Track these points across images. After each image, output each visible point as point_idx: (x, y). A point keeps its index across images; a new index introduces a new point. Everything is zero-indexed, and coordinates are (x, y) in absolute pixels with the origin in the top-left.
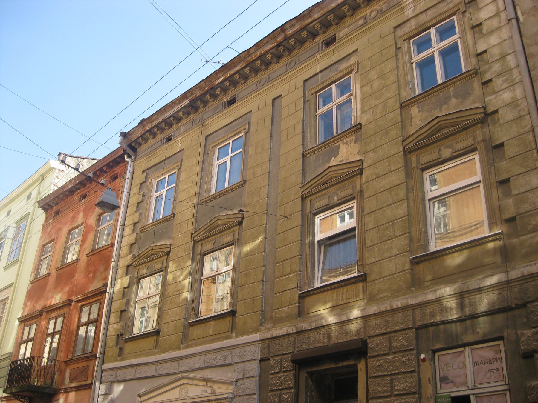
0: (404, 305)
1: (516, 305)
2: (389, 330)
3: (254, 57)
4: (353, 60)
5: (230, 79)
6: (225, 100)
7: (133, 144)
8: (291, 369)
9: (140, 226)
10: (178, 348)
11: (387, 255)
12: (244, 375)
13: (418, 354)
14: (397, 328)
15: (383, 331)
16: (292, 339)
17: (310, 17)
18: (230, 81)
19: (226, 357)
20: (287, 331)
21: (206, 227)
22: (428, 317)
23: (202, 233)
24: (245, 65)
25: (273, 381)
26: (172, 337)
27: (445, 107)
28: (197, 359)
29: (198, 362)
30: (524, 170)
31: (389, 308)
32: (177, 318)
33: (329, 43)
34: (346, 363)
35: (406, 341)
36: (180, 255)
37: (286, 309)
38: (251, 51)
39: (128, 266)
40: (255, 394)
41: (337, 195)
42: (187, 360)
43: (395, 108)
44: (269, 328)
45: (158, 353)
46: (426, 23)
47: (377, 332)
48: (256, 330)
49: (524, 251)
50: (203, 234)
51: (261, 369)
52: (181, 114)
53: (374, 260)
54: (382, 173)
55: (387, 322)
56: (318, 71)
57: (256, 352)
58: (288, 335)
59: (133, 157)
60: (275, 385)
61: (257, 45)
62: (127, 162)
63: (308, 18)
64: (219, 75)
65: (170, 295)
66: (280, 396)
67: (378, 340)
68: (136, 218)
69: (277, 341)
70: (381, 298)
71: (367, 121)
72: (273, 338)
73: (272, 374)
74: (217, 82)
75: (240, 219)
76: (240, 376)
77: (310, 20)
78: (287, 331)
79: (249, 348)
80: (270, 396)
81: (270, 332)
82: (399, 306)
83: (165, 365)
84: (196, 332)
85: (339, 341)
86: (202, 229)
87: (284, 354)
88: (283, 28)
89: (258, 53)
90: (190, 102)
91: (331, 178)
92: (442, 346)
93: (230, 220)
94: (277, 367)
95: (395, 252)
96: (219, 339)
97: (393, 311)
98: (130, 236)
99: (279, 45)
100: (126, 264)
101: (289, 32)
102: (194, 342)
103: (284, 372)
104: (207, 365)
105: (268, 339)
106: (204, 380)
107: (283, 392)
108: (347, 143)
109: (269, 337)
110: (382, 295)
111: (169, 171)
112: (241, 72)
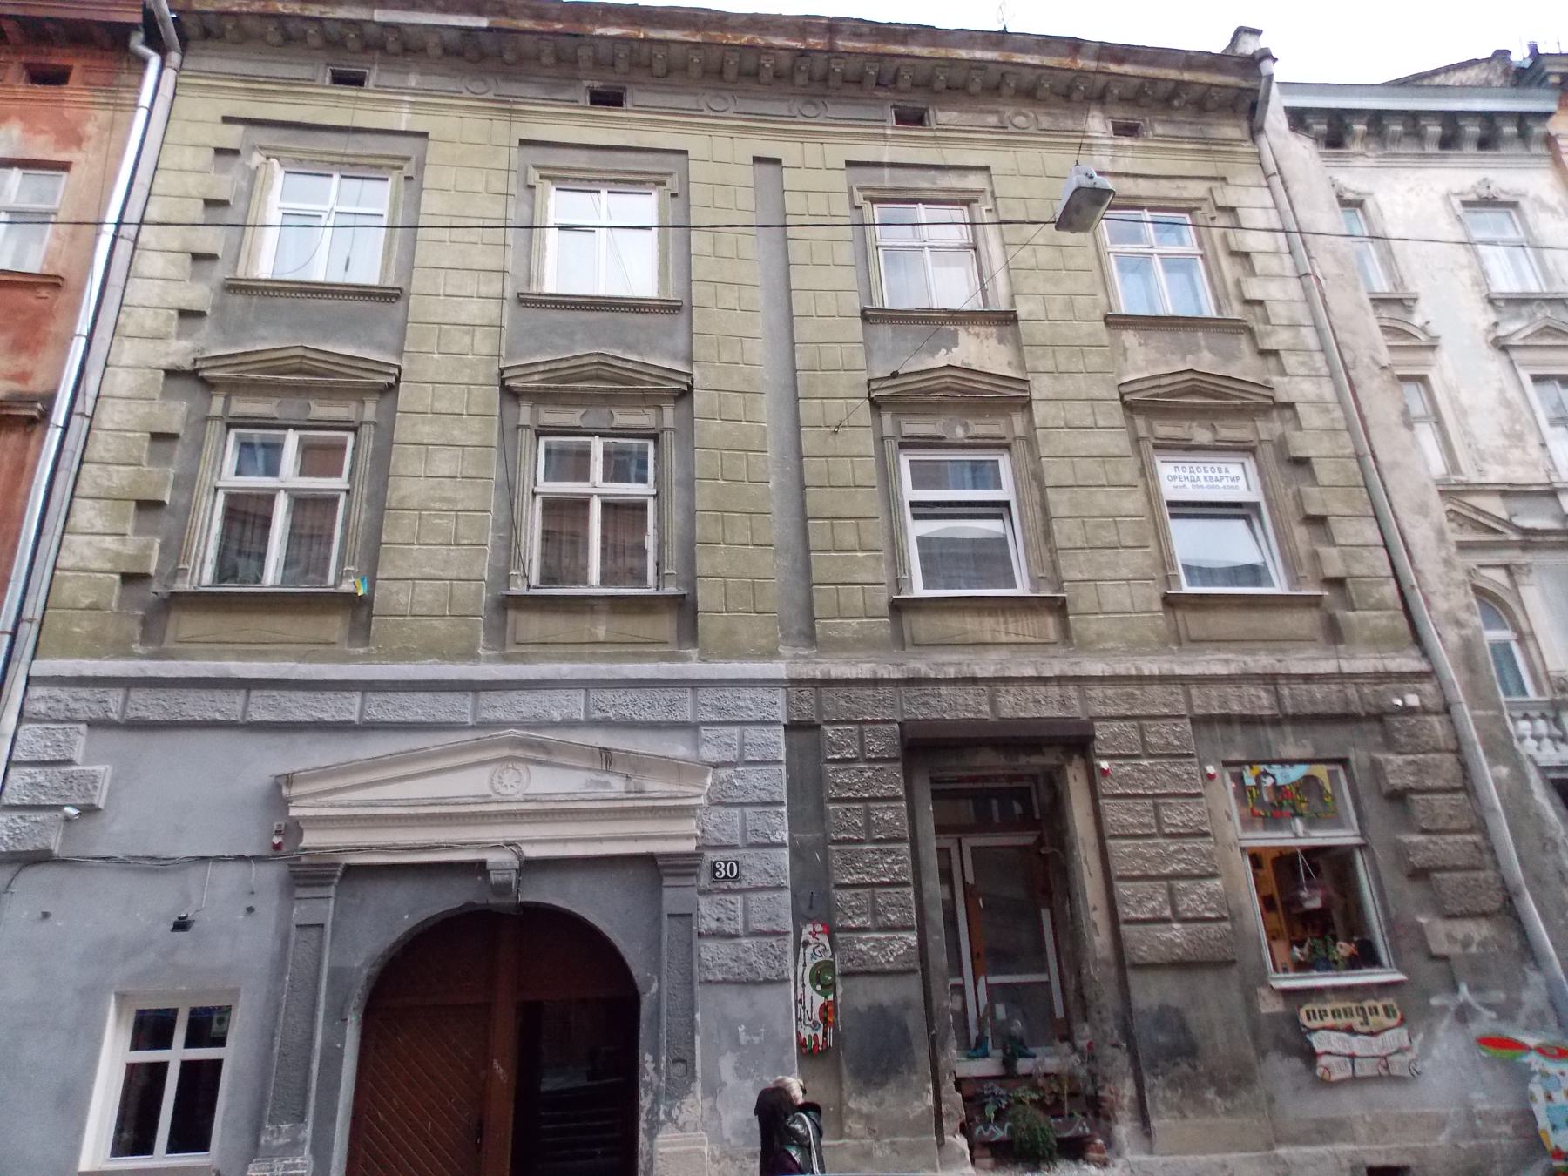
0: (1165, 672)
1: (1368, 714)
2: (1137, 712)
3: (730, 38)
4: (974, 182)
5: (636, 46)
6: (586, 83)
7: (188, 21)
8: (893, 755)
9: (220, 272)
10: (470, 655)
11: (1108, 573)
12: (742, 755)
13: (1202, 764)
14: (1154, 711)
15: (1123, 710)
16: (886, 692)
17: (904, 42)
18: (632, 50)
19: (671, 703)
20: (875, 672)
21: (553, 366)
22: (1215, 703)
23: (536, 377)
24: (698, 38)
25: (842, 777)
26: (436, 622)
27: (1189, 357)
28: (560, 696)
29: (573, 705)
30: (1350, 512)
31: (1133, 672)
32: (452, 574)
33: (912, 118)
34: (1036, 760)
35: (1177, 739)
36: (441, 406)
37: (854, 622)
38: (729, 22)
39: (170, 373)
40: (782, 803)
41: (966, 426)
42: (514, 696)
43: (1092, 317)
44: (805, 657)
45: (367, 659)
46: (1139, 198)
47: (1112, 711)
48: (771, 654)
49: (1367, 633)
50: (543, 381)
51: (789, 746)
52: (432, 41)
53: (1079, 576)
54: (1078, 423)
55: (1132, 696)
56: (886, 160)
57: (778, 706)
58: (875, 682)
59: (175, 57)
60: (849, 787)
61: (756, 22)
62: (144, 62)
63: (897, 42)
64: (612, 19)
65: (414, 503)
66: (868, 814)
67: (1116, 726)
68: (209, 240)
69: (843, 691)
70: (1104, 650)
71: (1030, 313)
72: (828, 682)
73: (833, 761)
74: (599, 31)
75: (685, 388)
76: (730, 756)
77: (902, 50)
78: (875, 672)
79: (748, 693)
80: (835, 811)
81: (822, 667)
82: (1157, 673)
83: (403, 698)
84: (533, 625)
85: (1022, 715)
86: (541, 368)
87: (865, 722)
88: (833, 26)
89: (745, 39)
90: (489, 30)
91: (947, 389)
92: (1243, 758)
93: (646, 378)
94: (849, 745)
95: (1125, 573)
96: (639, 657)
97: (1141, 680)
98: (172, 284)
99: (803, 53)
100: (165, 362)
101: (842, 44)
102: (530, 649)
103: (870, 760)
104: (598, 715)
105: (812, 682)
106: (607, 757)
107: (872, 805)
108: (977, 335)
109: (819, 675)
110: (1110, 644)
111: (352, 165)
112: (674, 48)
